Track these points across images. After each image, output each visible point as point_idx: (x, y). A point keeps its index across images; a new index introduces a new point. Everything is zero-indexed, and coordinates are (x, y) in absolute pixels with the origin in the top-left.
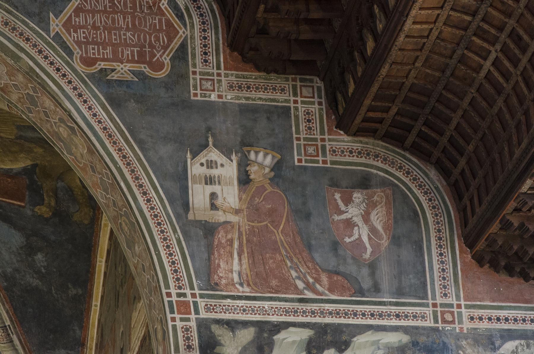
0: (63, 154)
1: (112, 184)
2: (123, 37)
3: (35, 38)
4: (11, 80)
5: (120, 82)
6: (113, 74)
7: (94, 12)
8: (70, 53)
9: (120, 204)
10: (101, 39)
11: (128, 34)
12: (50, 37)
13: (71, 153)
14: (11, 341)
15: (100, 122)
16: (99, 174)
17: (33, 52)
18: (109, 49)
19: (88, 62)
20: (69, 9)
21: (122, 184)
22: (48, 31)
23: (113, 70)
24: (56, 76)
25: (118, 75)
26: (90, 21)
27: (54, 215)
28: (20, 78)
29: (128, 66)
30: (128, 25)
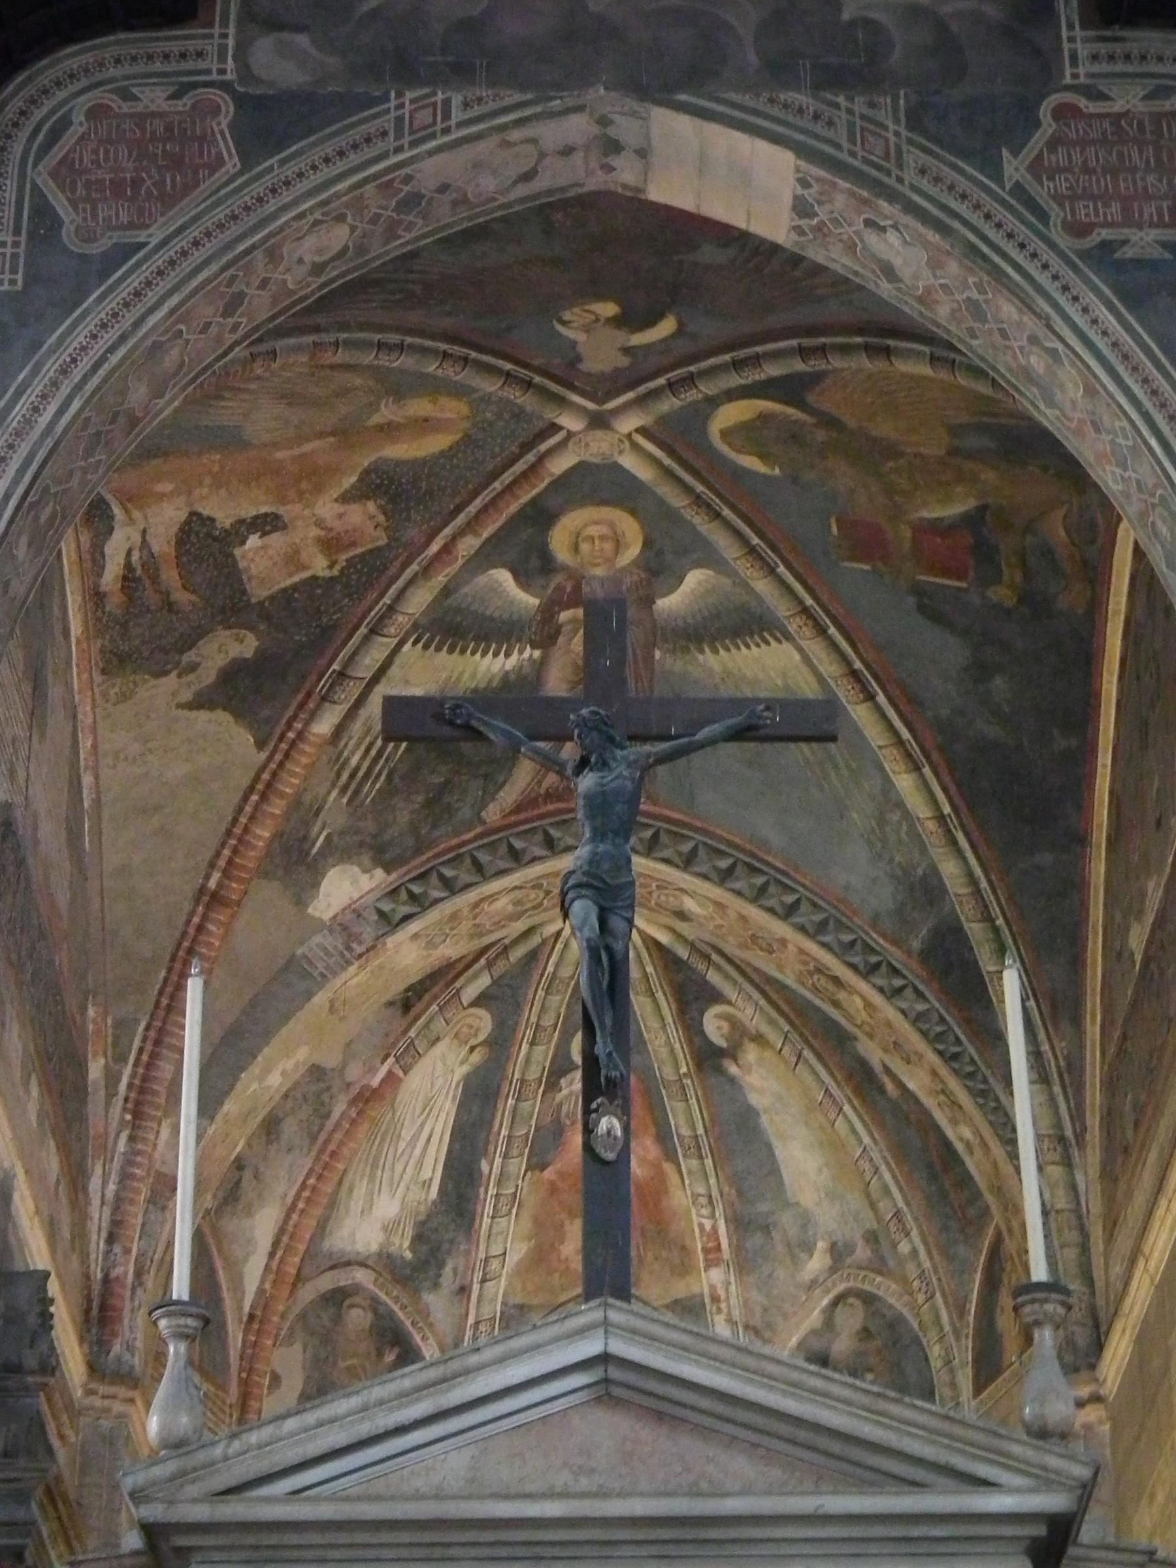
0: (1037, 407)
1: (1134, 449)
2: (1139, 183)
3: (977, 194)
4: (935, 276)
5: (1138, 263)
6: (1125, 248)
7: (1083, 143)
8: (1043, 216)
9: (1150, 482)
10: (1099, 188)
11: (1151, 179)
12: (1003, 189)
13: (1051, 403)
14: (954, 842)
15: (1105, 333)
16: (1109, 433)
17: (975, 218)
18: (1115, 208)
19: (1079, 230)
20: (1038, 140)
21: (1153, 442)
22: (999, 180)
23: (1125, 242)
24: (1020, 258)
25: (1136, 249)
26: (1077, 158)
27: (1021, 600)
28: (953, 267)
29: (1153, 234)
30: (1148, 162)
